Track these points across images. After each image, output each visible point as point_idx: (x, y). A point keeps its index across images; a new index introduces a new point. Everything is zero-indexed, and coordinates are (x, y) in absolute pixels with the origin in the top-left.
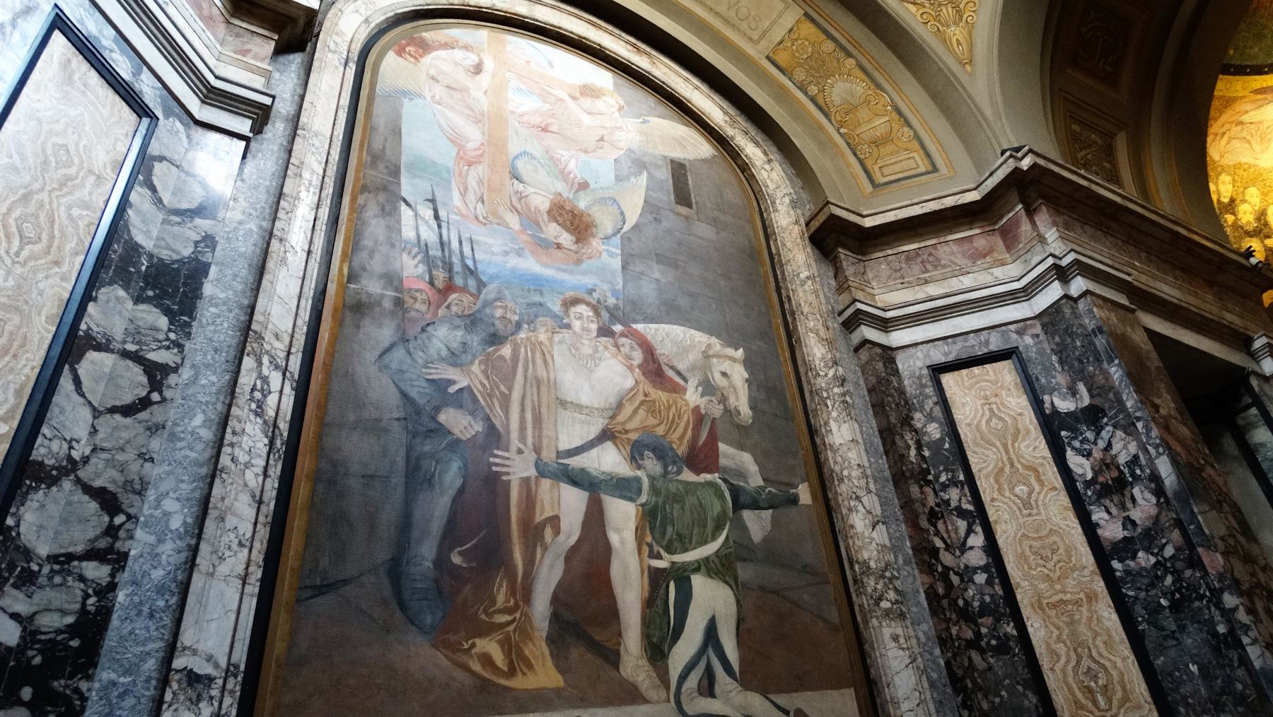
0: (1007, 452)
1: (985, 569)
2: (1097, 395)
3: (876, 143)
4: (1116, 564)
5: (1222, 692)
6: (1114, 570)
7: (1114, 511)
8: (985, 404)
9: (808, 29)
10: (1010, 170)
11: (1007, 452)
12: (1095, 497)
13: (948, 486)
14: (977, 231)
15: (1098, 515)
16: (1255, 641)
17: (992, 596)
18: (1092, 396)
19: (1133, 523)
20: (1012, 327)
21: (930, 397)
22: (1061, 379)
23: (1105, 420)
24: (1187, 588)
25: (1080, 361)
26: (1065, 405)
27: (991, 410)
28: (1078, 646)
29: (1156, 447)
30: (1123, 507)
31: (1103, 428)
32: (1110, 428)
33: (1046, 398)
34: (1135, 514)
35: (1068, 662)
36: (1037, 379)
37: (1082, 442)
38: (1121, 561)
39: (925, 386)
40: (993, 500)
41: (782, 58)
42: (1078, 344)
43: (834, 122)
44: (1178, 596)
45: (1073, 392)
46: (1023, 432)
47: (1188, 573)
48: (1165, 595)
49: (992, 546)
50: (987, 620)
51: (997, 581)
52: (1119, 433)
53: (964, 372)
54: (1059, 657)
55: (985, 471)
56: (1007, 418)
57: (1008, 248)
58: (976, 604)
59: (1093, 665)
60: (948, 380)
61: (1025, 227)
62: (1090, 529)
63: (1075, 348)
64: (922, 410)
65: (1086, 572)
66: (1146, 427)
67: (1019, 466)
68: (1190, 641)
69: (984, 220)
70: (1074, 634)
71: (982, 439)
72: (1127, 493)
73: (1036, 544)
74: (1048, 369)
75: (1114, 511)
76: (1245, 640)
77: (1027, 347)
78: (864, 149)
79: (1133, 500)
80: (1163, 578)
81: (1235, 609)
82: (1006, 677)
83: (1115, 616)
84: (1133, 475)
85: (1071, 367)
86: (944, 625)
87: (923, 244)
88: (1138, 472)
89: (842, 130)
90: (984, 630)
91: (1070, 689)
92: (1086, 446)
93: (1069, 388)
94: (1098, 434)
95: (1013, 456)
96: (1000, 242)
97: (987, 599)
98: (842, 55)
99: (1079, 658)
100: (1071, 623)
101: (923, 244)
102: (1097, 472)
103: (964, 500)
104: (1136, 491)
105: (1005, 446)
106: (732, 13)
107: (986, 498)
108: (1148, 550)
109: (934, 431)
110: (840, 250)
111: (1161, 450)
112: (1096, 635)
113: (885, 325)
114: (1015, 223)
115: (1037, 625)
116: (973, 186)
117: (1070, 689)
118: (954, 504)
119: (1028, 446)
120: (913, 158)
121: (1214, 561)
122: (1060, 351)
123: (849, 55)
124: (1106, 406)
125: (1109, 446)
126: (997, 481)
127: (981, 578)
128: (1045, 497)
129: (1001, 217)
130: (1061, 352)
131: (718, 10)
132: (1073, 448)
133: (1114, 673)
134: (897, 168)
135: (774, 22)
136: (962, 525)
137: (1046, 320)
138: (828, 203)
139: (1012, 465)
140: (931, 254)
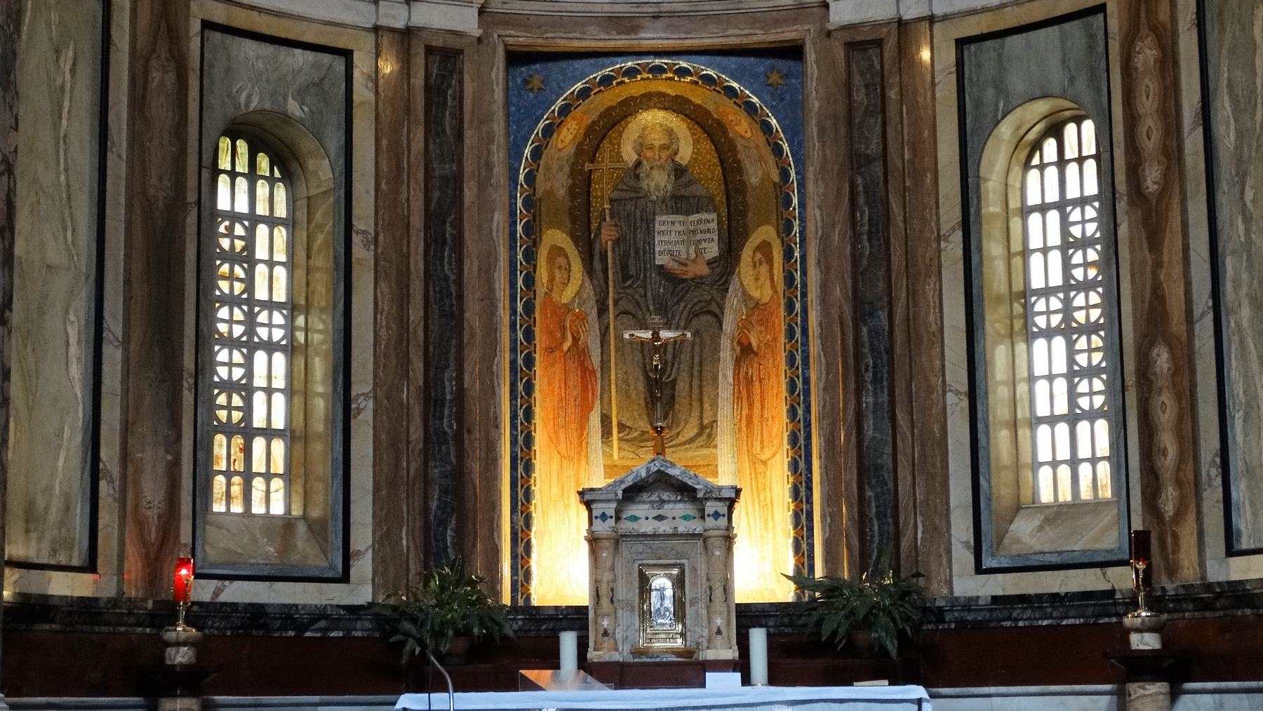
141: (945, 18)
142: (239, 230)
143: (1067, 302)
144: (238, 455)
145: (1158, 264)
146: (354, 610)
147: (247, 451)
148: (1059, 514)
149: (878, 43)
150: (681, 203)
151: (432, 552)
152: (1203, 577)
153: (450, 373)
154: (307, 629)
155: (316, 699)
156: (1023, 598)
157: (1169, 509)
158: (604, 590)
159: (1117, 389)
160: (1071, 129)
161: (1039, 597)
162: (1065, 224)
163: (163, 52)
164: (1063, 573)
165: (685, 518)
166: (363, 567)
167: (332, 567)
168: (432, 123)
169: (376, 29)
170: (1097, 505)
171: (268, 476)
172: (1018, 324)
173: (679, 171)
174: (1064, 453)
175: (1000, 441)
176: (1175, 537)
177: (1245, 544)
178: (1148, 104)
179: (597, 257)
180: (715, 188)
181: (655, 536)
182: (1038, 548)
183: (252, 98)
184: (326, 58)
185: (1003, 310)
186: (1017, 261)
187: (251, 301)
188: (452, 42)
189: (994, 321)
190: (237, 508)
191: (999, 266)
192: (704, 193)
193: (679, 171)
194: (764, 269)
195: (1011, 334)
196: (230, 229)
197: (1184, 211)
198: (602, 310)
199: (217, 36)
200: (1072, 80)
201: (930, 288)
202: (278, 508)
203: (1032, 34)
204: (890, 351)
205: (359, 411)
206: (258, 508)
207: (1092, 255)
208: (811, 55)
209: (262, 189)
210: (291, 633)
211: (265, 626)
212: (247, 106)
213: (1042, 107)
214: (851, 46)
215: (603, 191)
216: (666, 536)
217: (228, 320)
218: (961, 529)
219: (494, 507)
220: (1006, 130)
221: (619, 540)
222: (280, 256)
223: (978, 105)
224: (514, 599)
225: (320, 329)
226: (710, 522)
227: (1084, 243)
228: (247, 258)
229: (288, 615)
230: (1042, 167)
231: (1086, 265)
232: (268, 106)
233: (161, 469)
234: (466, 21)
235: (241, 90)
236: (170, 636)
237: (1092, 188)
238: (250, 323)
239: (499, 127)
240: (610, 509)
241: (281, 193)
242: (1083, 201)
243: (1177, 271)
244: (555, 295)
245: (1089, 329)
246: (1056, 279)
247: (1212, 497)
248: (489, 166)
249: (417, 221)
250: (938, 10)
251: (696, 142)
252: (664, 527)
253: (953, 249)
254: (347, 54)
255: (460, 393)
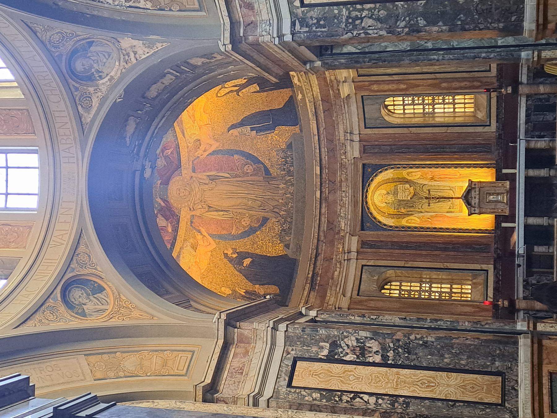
0: (335, 377)
1: (377, 398)
2: (328, 339)
3: (165, 364)
4: (389, 362)
5: (439, 352)
6: (391, 364)
7: (371, 355)
8: (312, 376)
9: (92, 359)
10: (223, 323)
11: (335, 377)
12: (364, 358)
13: (341, 399)
14: (233, 350)
15: (371, 360)
16: (427, 337)
17: (388, 400)
18: (327, 342)
19: (377, 351)
20: (284, 355)
21: (301, 392)
22: (314, 349)
23: (338, 342)
24: (405, 346)
25: (313, 339)
26: (326, 352)
27: (315, 375)
28: (413, 384)
29: (355, 333)
30: (370, 352)
31: (341, 345)
32: (342, 342)
33: (319, 356)
34: (375, 349)
35: (417, 388)
36: (310, 356)
37: (342, 353)
38: (389, 360)
39: (296, 391)
40: (352, 388)
41: (99, 375)
42: (306, 337)
43: (142, 375)
44: (406, 350)
45: (322, 348)
46: (329, 369)
47: (401, 343)
48: (404, 354)
49: (371, 394)
50: (396, 405)
51: (383, 397)
52: (346, 340)
53: (295, 377)
54: (415, 390)
55: (340, 386)
56: (321, 372)
57: (249, 343)
58: (389, 406)
59: (420, 382)
60: (294, 384)
61: (246, 333)
62: (374, 364)
63: (306, 338)
64: (305, 396)
65: (389, 372)
66: (347, 332)
67: (342, 375)
68: (421, 354)
69: (230, 345)
70: (408, 384)
71: (326, 382)
72: (366, 348)
73: (373, 382)
74: (308, 351)
75: (371, 355)
76: (425, 339)
77: (295, 354)
78: (163, 371)
79: (370, 347)
80: (399, 352)
81: (416, 337)
82: (417, 407)
83: (406, 370)
84: (362, 343)
85: (312, 344)
86: (396, 414)
87: (227, 369)
88: (362, 341)
89: (148, 375)
90: (400, 407)
91: (426, 391)
92: (344, 353)
93: (319, 349)
94: (341, 347)
95: (338, 375)
96: (242, 345)
97: (389, 402)
98: (113, 355)
99: (417, 385)
100: (405, 383)
101: (227, 369)
102: (355, 354)
103: (349, 396)
104: (368, 345)
105: (332, 376)
106: (67, 378)
107: (351, 390)
108: (388, 352)
109: (316, 395)
110: (215, 395)
111: (357, 332)
112: (410, 377)
113: (260, 393)
114: (241, 335)
115: (402, 392)
116: (216, 340)
117: (426, 391)
118: (349, 399)
119: (336, 370)
120: (181, 357)
121: (399, 335)
122: (303, 344)
123: (116, 352)
124: (334, 339)
125: (347, 345)
126: (345, 384)
127: (380, 401)
128: (356, 371)
129: (234, 339)
130: (304, 344)
131: (61, 382)
132: (343, 356)
133: (424, 378)
134: (182, 364)
135: (81, 368)
136: (358, 399)
137: (288, 343)
138: (196, 386)
139: (341, 377)
140: (234, 369)
141: (359, 131)
142: (403, 293)
143: (427, 104)
144: (457, 295)
145: (423, 85)
146: (494, 269)
147: (455, 293)
148: (477, 107)
149: (364, 146)
150: (396, 193)
151: (481, 251)
152: (495, 77)
153: (438, 245)
154: (499, 279)
155: (516, 277)
156: (497, 116)
157: (479, 84)
158: (492, 211)
159: (448, 94)
160: (386, 103)
161: (497, 112)
162: (409, 105)
163: (365, 303)
164: (492, 107)
165: (475, 192)
166: (484, 267)
167: (484, 273)
168: (379, 248)
169: (357, 259)
170: (475, 98)
171: (462, 289)
172: (431, 115)
173: (388, 193)
174: (462, 105)
175: (458, 120)
176: (486, 82)
177: (488, 68)
178: (386, 87)
179: (408, 213)
180: (393, 185)
181: (479, 199)
182: (485, 112)
183: (374, 286)
184: (363, 270)
185: (427, 119)
186: (416, 115)
187: (420, 291)
188: (360, 242)
189: (431, 121)
190: (470, 296)
191: (417, 119)
192: (393, 188)
193: (388, 193)
194: (413, 174)
195: (434, 117)
196: (403, 294)
197: (411, 80)
198: (421, 212)
199: (360, 293)
200: (377, 103)
201: (422, 135)
202: (470, 287)
203: (366, 112)
204: (436, 145)
205: (447, 266)
206: (470, 291)
207: (416, 99)
208: (365, 162)
209: (393, 287)
210: (500, 282)
211: (499, 287)
212: (375, 287)
213: (382, 110)
214: (364, 152)
215: (392, 211)
216: (479, 196)
217: (425, 295)
218: (480, 129)
219: (471, 236)
220: (387, 118)
221: (480, 207)
222: (409, 284)
223: (380, 124)
224: (493, 233)
225: (426, 274)
226: (477, 186)
227: (413, 100)
228: (409, 291)
229: (496, 282)
230: (394, 110)
231: (418, 100)
232: (375, 283)
233: (462, 308)
234: (355, 239)
235: (372, 289)
236: (501, 305)
237: (401, 98)
238: (425, 291)
239: (380, 233)
240: (473, 209)
241: (393, 283)
242: (403, 100)
243: (425, 81)
244: (418, 223)
245: (433, 100)
246: (421, 107)
247: (477, 74)
248: (389, 235)
249: (402, 251)
250: (358, 132)
251: (381, 189)
252: (477, 197)
253: (413, 130)
254: (363, 266)
255: (443, 243)
